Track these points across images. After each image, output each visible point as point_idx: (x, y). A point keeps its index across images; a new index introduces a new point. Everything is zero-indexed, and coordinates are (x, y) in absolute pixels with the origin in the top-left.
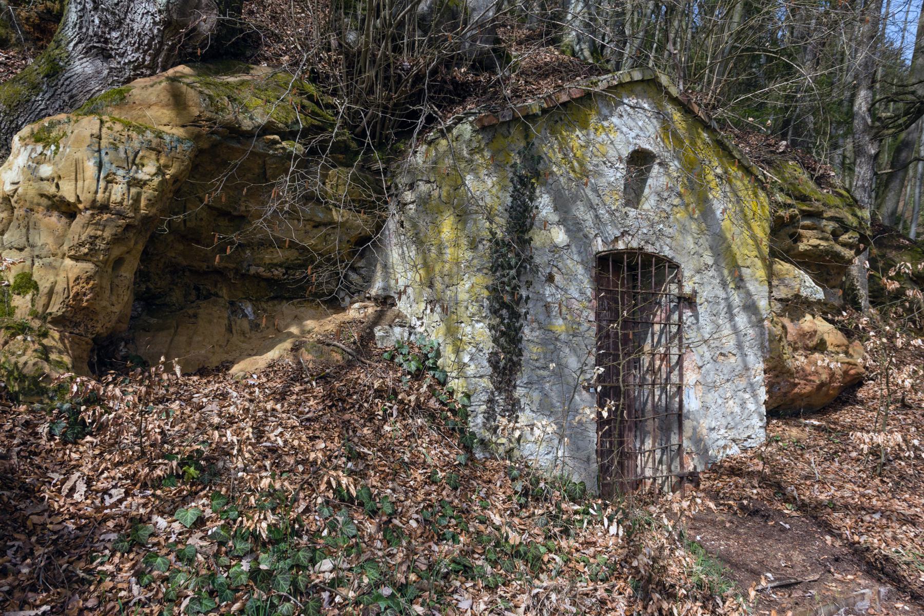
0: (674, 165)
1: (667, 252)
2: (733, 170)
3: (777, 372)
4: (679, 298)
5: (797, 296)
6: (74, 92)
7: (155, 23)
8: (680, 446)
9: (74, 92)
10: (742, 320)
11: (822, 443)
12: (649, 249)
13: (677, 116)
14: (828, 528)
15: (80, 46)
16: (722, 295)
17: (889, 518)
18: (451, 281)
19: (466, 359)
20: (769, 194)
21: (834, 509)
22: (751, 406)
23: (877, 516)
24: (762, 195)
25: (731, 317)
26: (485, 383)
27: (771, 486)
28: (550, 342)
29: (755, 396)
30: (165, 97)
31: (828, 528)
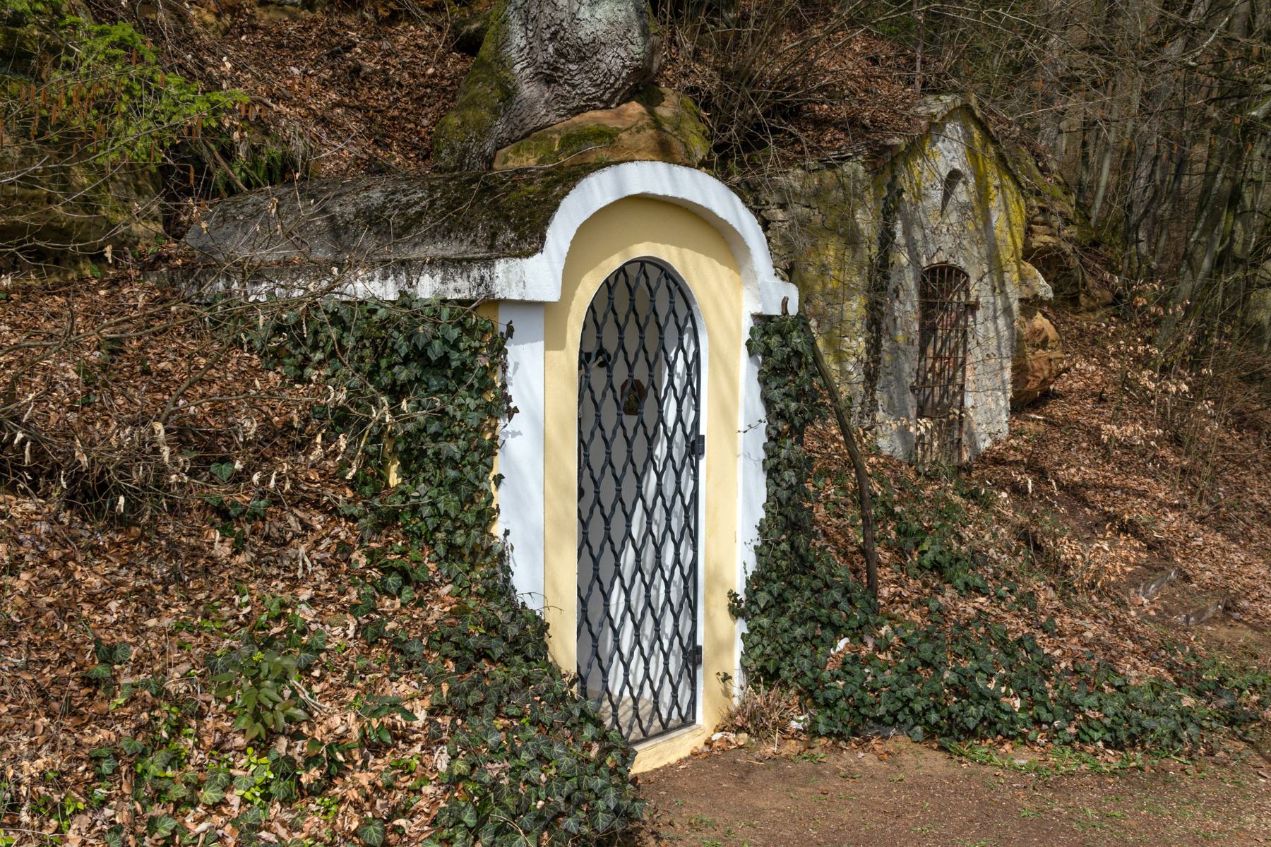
0: (972, 181)
1: (962, 264)
2: (1007, 180)
3: (1020, 371)
4: (966, 306)
5: (1036, 296)
6: (524, 115)
7: (624, 67)
8: (960, 440)
9: (524, 115)
10: (1001, 322)
11: (1058, 435)
12: (952, 262)
13: (977, 135)
14: (1085, 503)
15: (528, 71)
16: (992, 300)
17: (1127, 493)
18: (835, 297)
19: (850, 368)
20: (1026, 199)
21: (1087, 489)
22: (1002, 403)
23: (1118, 492)
24: (1022, 201)
25: (995, 318)
26: (861, 388)
27: (1035, 472)
28: (896, 350)
29: (1005, 393)
30: (652, 144)
31: (1085, 503)
